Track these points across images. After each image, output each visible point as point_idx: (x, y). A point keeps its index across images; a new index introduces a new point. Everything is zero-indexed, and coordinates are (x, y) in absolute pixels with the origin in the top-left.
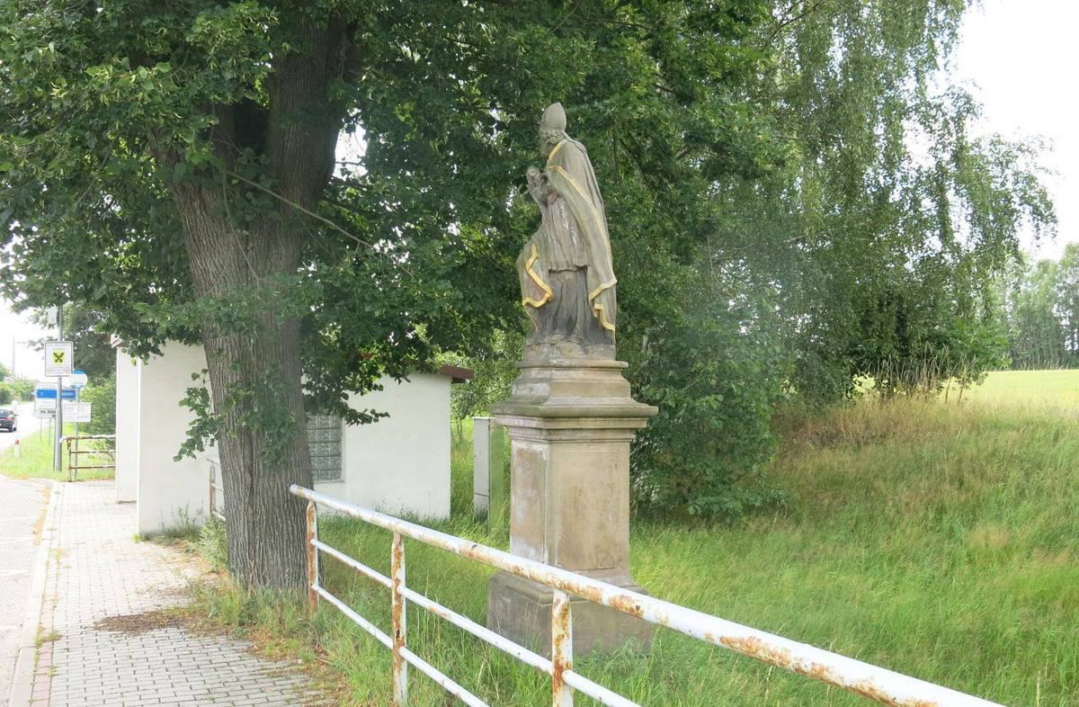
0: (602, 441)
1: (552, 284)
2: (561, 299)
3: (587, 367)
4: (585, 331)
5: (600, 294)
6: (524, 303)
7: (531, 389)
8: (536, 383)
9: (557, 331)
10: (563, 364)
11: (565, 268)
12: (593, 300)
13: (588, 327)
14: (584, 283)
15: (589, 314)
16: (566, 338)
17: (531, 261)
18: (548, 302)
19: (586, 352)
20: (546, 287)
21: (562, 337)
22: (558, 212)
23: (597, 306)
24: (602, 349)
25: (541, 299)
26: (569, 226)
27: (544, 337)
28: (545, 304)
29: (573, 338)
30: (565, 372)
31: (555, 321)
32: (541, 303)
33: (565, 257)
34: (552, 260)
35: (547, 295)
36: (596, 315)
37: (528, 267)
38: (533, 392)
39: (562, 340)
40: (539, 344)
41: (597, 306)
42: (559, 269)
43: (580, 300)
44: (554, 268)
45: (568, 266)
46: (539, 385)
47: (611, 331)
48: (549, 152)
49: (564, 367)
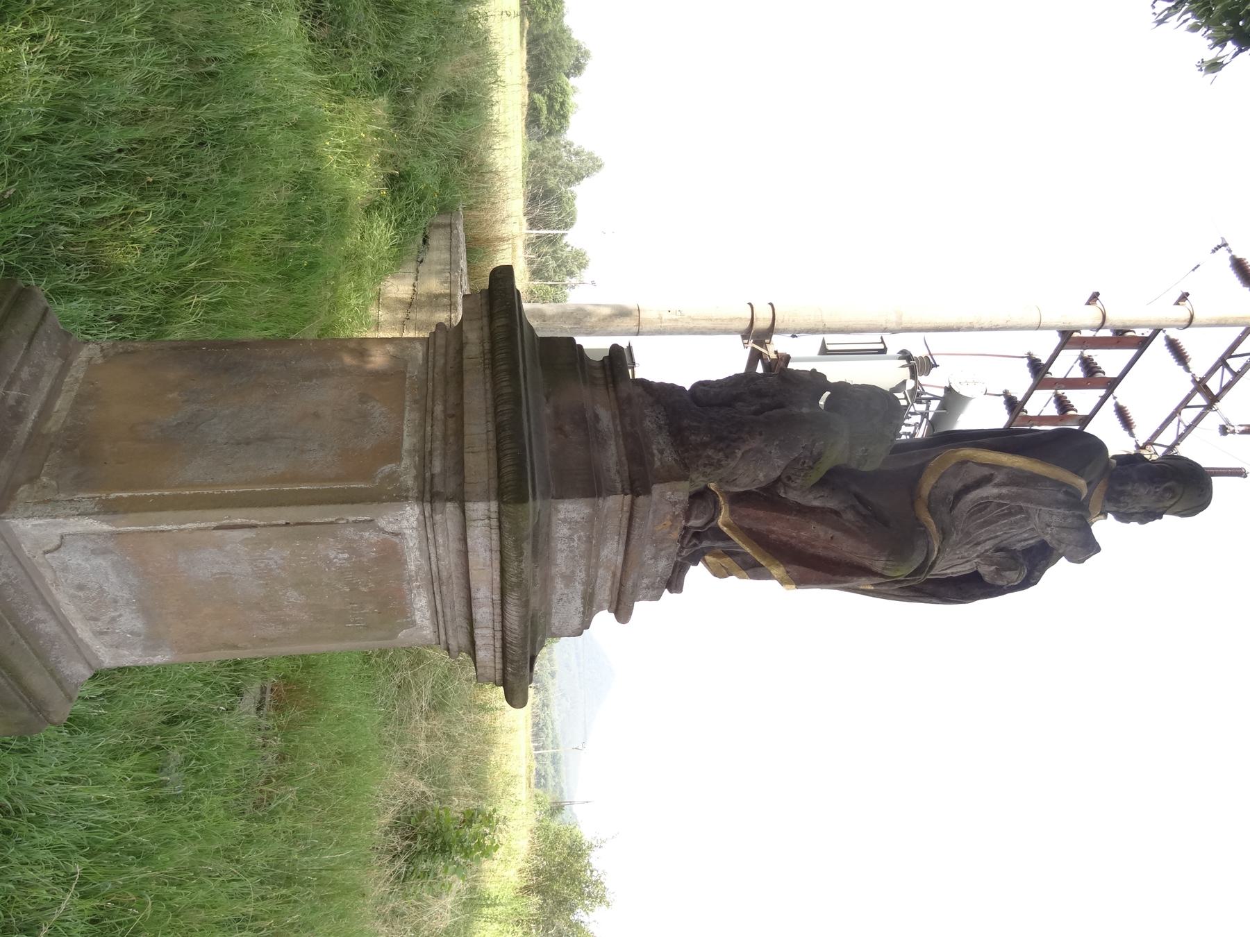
7: (569, 579)
38: (559, 585)
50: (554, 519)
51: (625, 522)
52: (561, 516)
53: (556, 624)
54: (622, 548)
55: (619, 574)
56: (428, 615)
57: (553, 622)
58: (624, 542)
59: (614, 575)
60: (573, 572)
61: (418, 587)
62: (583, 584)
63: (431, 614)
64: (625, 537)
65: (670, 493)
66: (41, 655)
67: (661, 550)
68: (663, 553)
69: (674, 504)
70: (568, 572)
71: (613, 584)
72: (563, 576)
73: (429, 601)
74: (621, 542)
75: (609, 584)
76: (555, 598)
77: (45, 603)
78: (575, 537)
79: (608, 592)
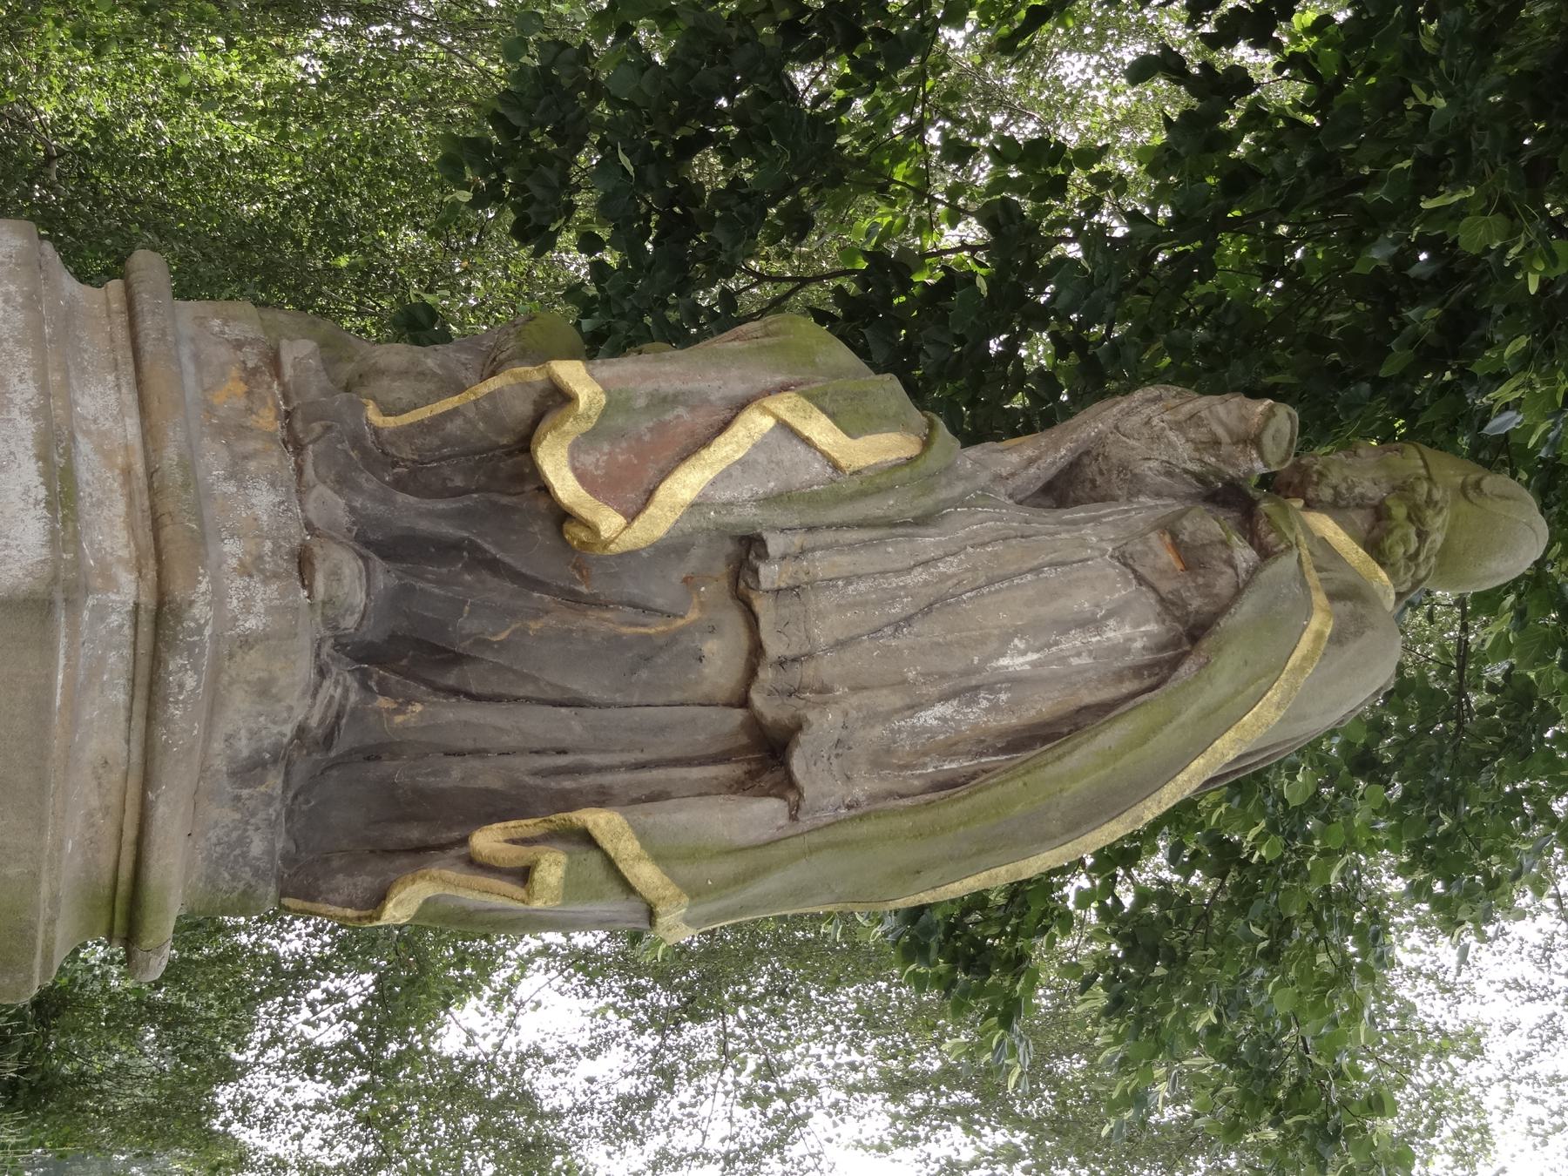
1: (670, 549)
2: (575, 600)
3: (147, 781)
4: (372, 754)
5: (628, 888)
6: (571, 373)
8: (43, 457)
9: (385, 577)
10: (175, 663)
11: (775, 647)
12: (586, 838)
13: (396, 771)
14: (668, 752)
15: (487, 776)
16: (339, 645)
17: (820, 430)
18: (563, 516)
19: (248, 771)
20: (658, 521)
21: (349, 623)
22: (1081, 602)
23: (552, 868)
24: (257, 847)
25: (582, 477)
26: (1015, 681)
27: (343, 483)
28: (545, 489)
29: (342, 687)
30: (117, 662)
31: (446, 550)
32: (566, 487)
33: (840, 645)
34: (823, 565)
35: (609, 522)
36: (488, 840)
37: (784, 406)
39: (331, 623)
40: (295, 445)
41: (552, 868)
42: (761, 605)
43: (569, 726)
44: (770, 574)
45: (782, 663)
46: (28, 472)
47: (379, 899)
48: (1334, 507)
49: (157, 660)
51: (122, 335)
54: (130, 397)
55: (139, 468)
58: (132, 380)
59: (127, 472)
62: (34, 414)
64: (131, 368)
65: (218, 322)
67: (246, 457)
68: (252, 466)
69: (238, 345)
74: (123, 381)
75: (120, 507)
79: (122, 536)
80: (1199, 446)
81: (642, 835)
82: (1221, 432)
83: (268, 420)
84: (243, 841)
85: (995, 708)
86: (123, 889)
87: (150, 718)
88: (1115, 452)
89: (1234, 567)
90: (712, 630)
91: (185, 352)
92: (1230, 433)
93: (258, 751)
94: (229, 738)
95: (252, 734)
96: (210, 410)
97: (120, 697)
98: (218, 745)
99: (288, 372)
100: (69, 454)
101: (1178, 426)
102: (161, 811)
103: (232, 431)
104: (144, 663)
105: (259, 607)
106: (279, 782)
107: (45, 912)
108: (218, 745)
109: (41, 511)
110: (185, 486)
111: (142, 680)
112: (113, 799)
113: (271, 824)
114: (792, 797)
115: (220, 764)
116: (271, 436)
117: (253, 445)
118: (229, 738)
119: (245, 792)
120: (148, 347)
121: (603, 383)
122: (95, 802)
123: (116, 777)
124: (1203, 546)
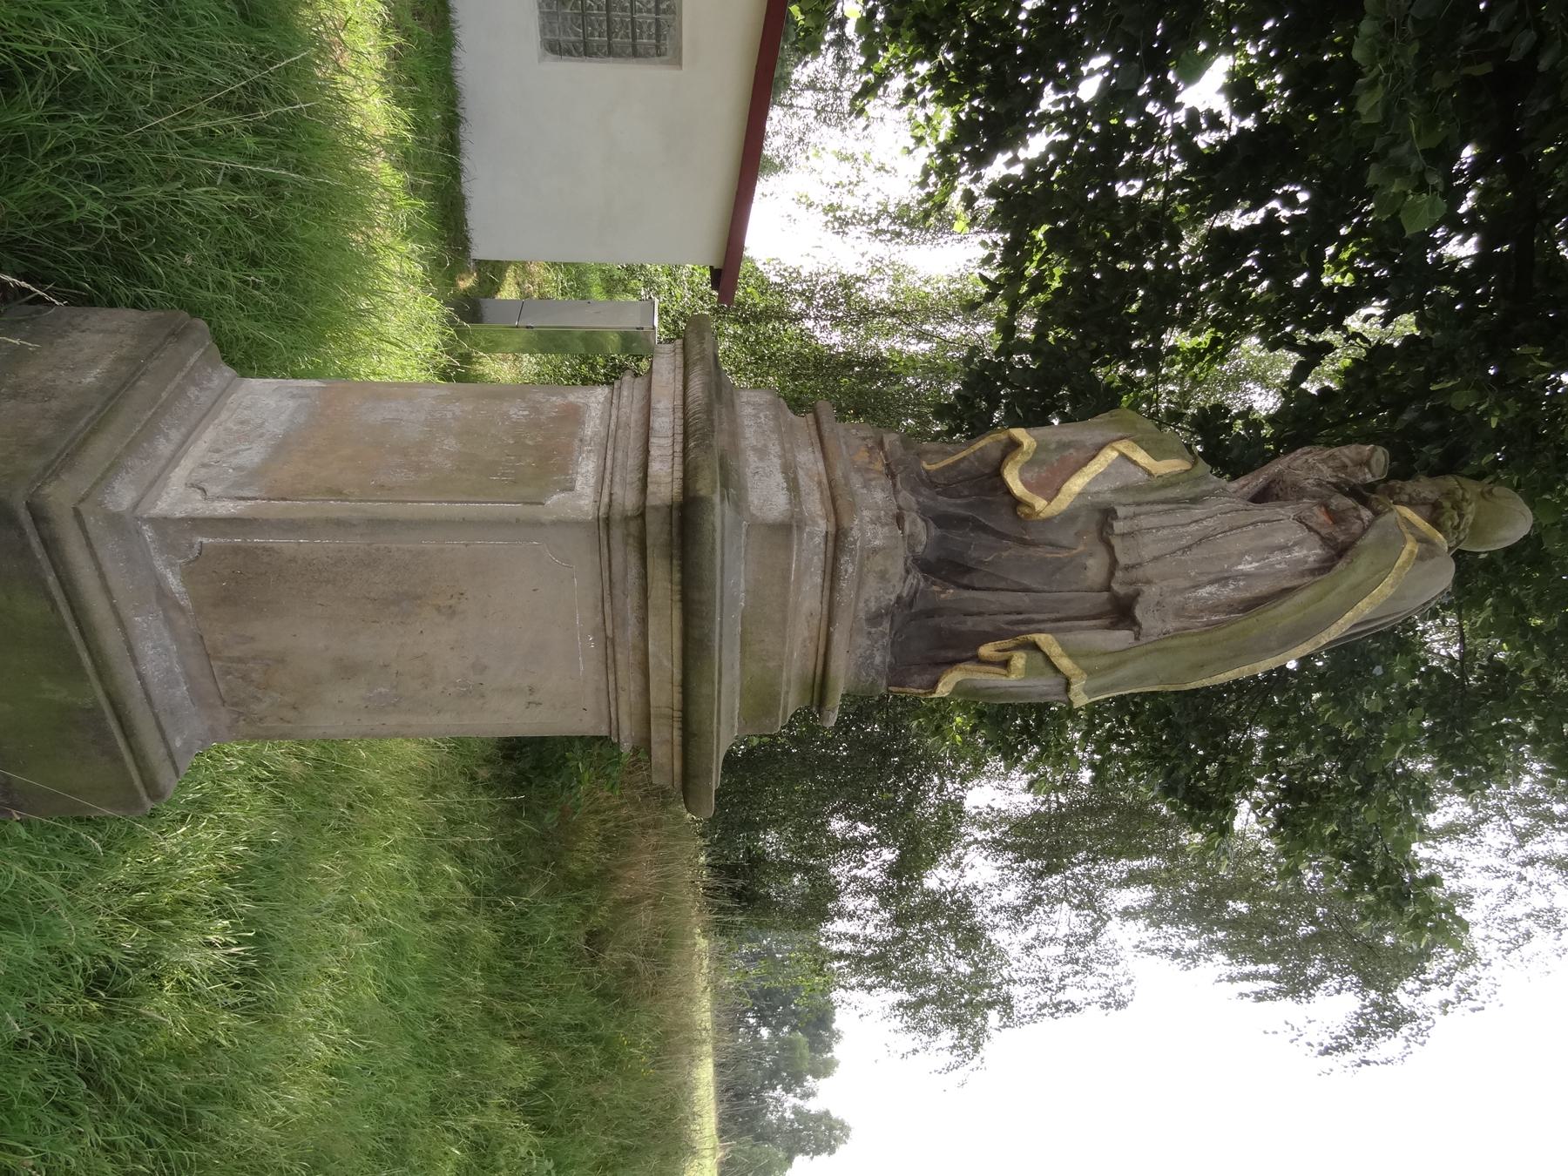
0: (609, 663)
1: (1069, 517)
2: (1024, 543)
3: (830, 622)
4: (930, 613)
5: (1056, 670)
6: (1019, 433)
7: (762, 452)
9: (935, 532)
10: (844, 559)
11: (1123, 560)
12: (1035, 647)
13: (942, 622)
14: (1071, 613)
15: (985, 625)
16: (915, 560)
17: (1141, 457)
18: (1017, 502)
19: (875, 619)
20: (1063, 502)
21: (920, 549)
22: (1280, 539)
23: (1019, 660)
24: (878, 660)
25: (1026, 484)
26: (1247, 575)
27: (914, 491)
28: (1008, 492)
29: (916, 579)
30: (817, 561)
31: (961, 522)
32: (1017, 488)
33: (1156, 559)
34: (1144, 522)
35: (1040, 503)
36: (986, 650)
37: (1123, 446)
38: (752, 458)
39: (911, 548)
40: (891, 474)
41: (1019, 660)
42: (1116, 542)
43: (1024, 600)
44: (1119, 526)
45: (1127, 568)
46: (779, 478)
47: (934, 685)
48: (1410, 504)
49: (836, 559)
50: (737, 402)
51: (814, 433)
52: (744, 400)
53: (756, 502)
54: (819, 455)
55: (825, 480)
56: (592, 481)
57: (750, 499)
59: (820, 483)
60: (765, 446)
61: (590, 451)
62: (780, 457)
63: (596, 482)
66: (131, 447)
68: (873, 483)
69: (864, 439)
70: (759, 446)
71: (822, 493)
72: (754, 449)
73: (598, 466)
75: (817, 496)
76: (749, 472)
77: (189, 434)
78: (761, 415)
80: (1335, 469)
81: (1062, 645)
82: (1347, 461)
83: (879, 466)
84: (872, 656)
85: (1237, 589)
86: (818, 679)
87: (832, 589)
88: (1288, 479)
89: (1362, 520)
90: (1091, 555)
91: (842, 440)
92: (1352, 460)
93: (879, 608)
94: (866, 601)
95: (877, 599)
96: (853, 463)
97: (819, 580)
98: (861, 605)
99: (887, 447)
100: (795, 473)
101: (1323, 461)
102: (836, 637)
103: (863, 470)
104: (830, 561)
105: (880, 536)
106: (888, 626)
107: (784, 688)
108: (861, 605)
109: (785, 492)
110: (846, 485)
111: (829, 571)
112: (815, 634)
113: (884, 648)
114: (1136, 629)
115: (862, 615)
116: (881, 472)
117: (872, 475)
118: (866, 601)
119: (873, 630)
120: (826, 434)
121: (1034, 437)
122: (806, 634)
123: (816, 622)
124: (1343, 511)
